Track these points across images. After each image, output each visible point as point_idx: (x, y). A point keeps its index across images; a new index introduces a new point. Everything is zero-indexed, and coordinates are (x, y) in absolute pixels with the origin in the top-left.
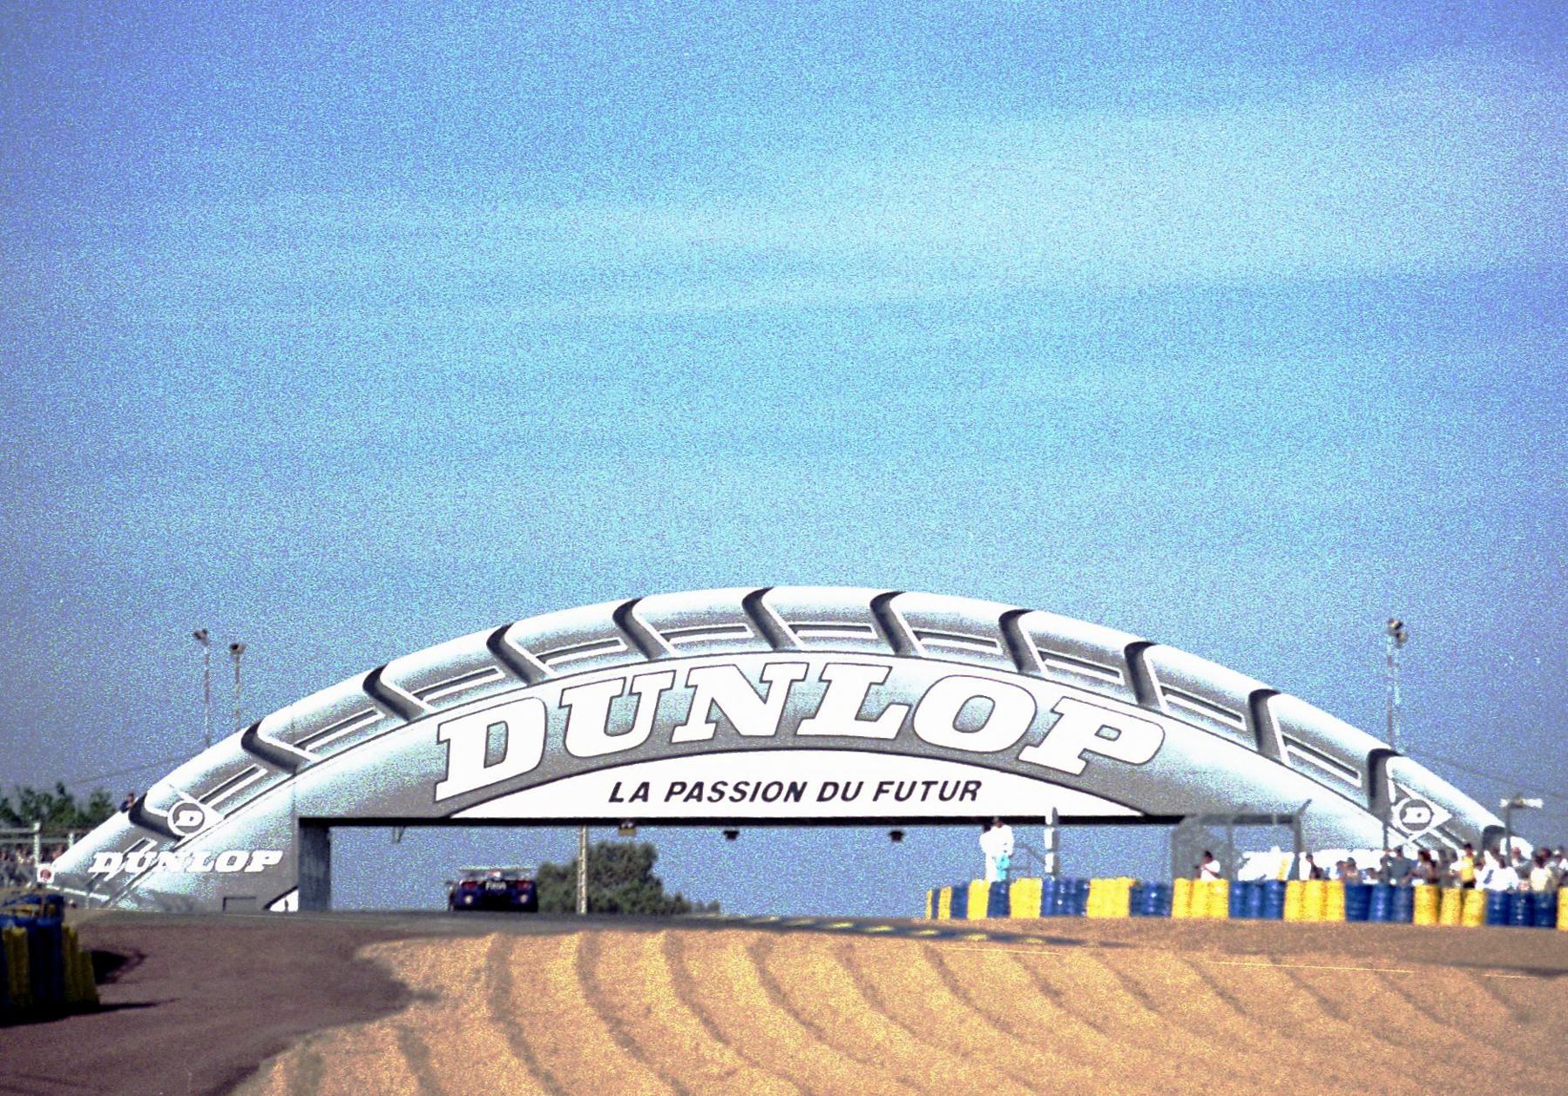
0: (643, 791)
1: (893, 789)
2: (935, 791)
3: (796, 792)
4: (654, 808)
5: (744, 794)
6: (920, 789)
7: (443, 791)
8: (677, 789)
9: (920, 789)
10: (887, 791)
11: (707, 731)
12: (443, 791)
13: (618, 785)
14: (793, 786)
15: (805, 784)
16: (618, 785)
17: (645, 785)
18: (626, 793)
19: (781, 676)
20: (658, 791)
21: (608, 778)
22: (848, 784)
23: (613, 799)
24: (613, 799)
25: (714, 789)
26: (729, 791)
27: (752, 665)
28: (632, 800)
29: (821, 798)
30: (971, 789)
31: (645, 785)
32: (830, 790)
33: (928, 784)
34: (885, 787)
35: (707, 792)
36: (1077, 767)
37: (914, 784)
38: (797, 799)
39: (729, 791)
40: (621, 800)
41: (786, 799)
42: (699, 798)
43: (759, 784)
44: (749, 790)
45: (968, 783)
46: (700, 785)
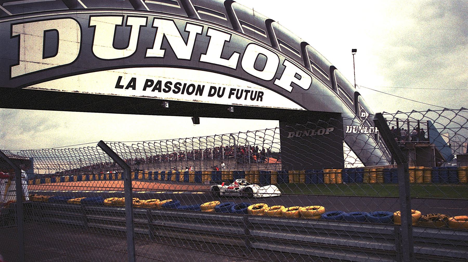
0: (132, 84)
1: (235, 92)
2: (249, 94)
3: (200, 90)
4: (138, 92)
5: (179, 89)
6: (244, 94)
7: (16, 72)
8: (149, 83)
9: (244, 94)
10: (233, 94)
11: (161, 53)
12: (16, 72)
13: (120, 78)
14: (199, 86)
15: (204, 86)
16: (120, 78)
17: (134, 80)
18: (125, 82)
19: (194, 30)
20: (140, 84)
21: (113, 75)
22: (220, 88)
23: (118, 86)
24: (118, 86)
25: (166, 85)
26: (173, 87)
27: (181, 22)
28: (127, 88)
29: (210, 95)
30: (260, 96)
31: (134, 80)
32: (213, 91)
33: (247, 92)
34: (233, 92)
35: (163, 87)
36: (290, 89)
37: (242, 90)
38: (201, 94)
39: (173, 87)
40: (122, 87)
41: (196, 94)
42: (160, 91)
43: (185, 84)
44: (181, 87)
45: (260, 92)
46: (159, 82)
